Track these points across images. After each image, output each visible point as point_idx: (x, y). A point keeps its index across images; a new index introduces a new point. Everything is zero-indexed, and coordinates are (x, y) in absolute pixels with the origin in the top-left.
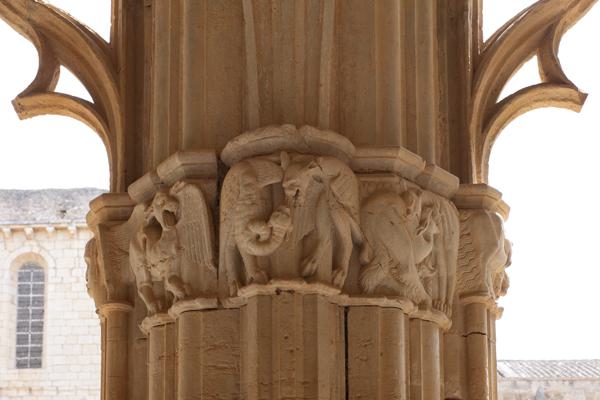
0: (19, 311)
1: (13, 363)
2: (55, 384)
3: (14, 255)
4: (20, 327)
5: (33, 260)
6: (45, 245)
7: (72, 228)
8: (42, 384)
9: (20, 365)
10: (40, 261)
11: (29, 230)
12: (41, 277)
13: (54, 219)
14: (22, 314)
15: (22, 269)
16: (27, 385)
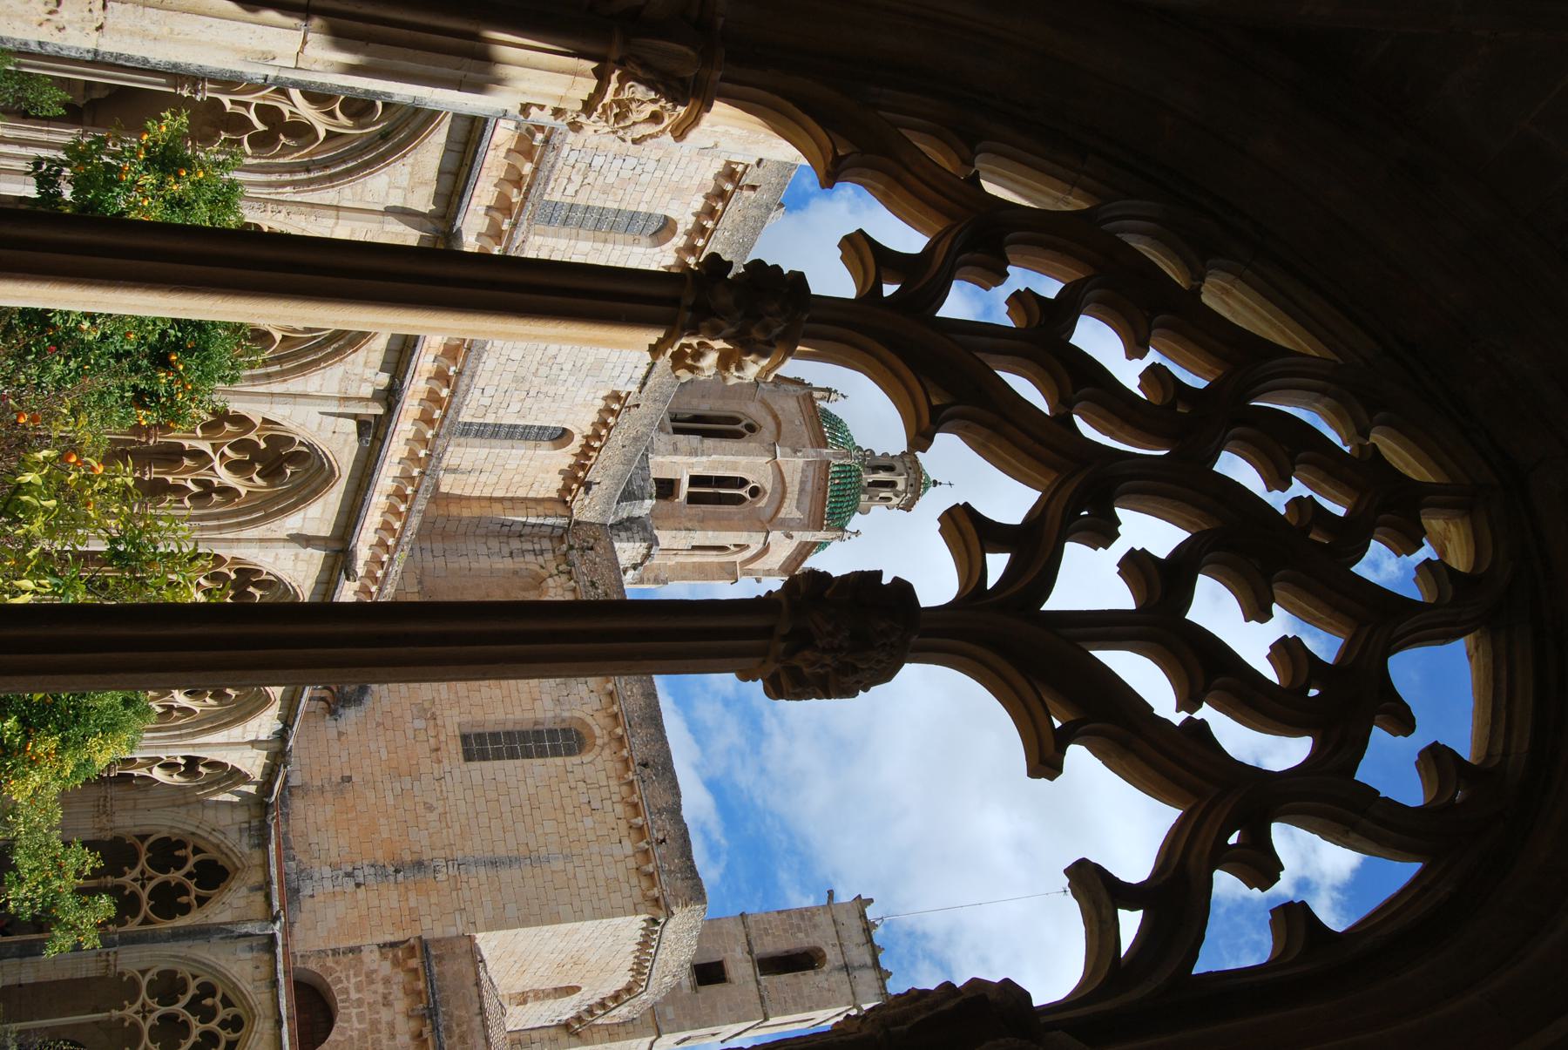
0: (528, 732)
1: (466, 730)
2: (447, 775)
3: (589, 720)
4: (509, 734)
5: (588, 741)
6: (607, 753)
7: (630, 776)
8: (446, 761)
9: (465, 738)
10: (588, 748)
11: (619, 731)
12: (570, 752)
13: (637, 757)
14: (524, 735)
15: (576, 731)
16: (443, 746)
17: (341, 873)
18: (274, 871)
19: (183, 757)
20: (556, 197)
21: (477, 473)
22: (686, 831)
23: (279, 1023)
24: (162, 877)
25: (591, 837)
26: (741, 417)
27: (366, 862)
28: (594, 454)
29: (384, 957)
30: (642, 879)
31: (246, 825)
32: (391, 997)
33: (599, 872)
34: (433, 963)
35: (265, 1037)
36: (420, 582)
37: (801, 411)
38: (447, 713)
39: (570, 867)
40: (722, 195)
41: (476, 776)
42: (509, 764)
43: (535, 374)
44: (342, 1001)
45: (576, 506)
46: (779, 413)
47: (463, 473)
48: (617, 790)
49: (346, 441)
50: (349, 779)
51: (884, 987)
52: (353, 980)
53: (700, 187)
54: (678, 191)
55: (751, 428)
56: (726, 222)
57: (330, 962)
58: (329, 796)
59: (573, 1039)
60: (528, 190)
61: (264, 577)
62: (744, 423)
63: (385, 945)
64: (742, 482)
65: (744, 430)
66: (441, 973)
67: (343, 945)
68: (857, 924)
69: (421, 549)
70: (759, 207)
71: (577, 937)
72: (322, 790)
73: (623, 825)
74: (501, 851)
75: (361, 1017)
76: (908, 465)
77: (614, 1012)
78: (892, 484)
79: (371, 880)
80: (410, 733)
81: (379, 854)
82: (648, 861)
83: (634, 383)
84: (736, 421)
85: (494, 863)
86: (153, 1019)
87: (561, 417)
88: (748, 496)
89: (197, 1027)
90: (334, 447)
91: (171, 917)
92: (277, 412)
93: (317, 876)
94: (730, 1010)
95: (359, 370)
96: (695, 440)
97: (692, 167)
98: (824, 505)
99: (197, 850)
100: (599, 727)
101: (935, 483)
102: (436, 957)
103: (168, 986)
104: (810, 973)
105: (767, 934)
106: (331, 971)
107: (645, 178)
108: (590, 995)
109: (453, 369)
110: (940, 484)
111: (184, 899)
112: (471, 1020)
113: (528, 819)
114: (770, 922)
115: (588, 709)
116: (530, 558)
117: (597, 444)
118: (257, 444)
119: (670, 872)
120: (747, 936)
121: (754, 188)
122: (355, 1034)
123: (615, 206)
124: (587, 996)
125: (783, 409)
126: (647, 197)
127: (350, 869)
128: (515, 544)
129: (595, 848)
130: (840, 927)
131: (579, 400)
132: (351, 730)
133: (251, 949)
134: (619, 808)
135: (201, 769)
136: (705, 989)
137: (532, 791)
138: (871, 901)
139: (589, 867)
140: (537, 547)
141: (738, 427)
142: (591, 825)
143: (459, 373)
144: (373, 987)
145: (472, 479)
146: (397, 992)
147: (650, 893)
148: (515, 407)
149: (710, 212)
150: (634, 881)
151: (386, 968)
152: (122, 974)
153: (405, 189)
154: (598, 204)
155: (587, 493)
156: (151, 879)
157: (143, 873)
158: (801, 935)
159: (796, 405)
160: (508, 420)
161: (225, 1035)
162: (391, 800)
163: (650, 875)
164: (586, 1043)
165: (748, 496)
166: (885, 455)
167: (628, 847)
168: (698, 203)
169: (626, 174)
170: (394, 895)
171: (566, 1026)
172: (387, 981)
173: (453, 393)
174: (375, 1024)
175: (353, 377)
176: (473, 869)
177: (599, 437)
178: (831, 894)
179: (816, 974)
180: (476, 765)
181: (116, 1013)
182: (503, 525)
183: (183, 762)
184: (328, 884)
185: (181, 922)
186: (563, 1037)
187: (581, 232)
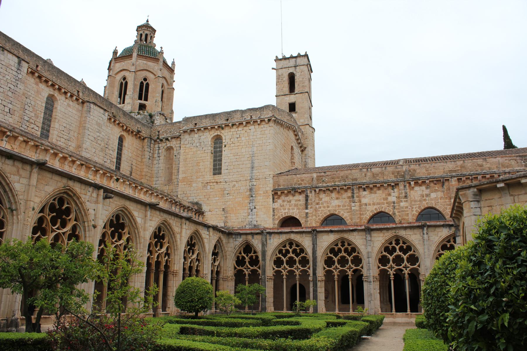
1: (212, 173)
3: (212, 136)
4: (214, 161)
8: (221, 180)
9: (214, 174)
14: (215, 157)
17: (251, 213)
18: (248, 232)
19: (212, 256)
20: (39, 133)
22: (249, 109)
23: (292, 232)
24: (247, 263)
25: (247, 138)
26: (120, 82)
27: (248, 205)
28: (128, 129)
29: (276, 202)
30: (262, 124)
31: (234, 239)
32: (288, 200)
33: (258, 137)
34: (280, 188)
35: (296, 236)
36: (166, 185)
38: (206, 179)
39: (256, 145)
40: (40, 77)
41: (226, 171)
42: (223, 161)
43: (100, 145)
44: (288, 214)
45: (145, 136)
46: (120, 69)
48: (234, 129)
49: (112, 203)
50: (223, 209)
51: (302, 56)
52: (282, 211)
53: (37, 84)
54: (38, 92)
55: (124, 79)
56: (50, 77)
57: (276, 217)
58: (228, 215)
59: (306, 150)
60: (29, 139)
61: (157, 230)
62: (123, 81)
63: (273, 201)
64: (142, 83)
65: (125, 81)
66: (283, 185)
67: (272, 213)
68: (283, 61)
69: (156, 184)
70: (45, 65)
71: (277, 145)
72: (226, 217)
73: (245, 128)
74: (249, 165)
75: (293, 209)
76: (141, 29)
77: (300, 137)
78: (146, 35)
79: (254, 204)
80: (212, 190)
81: (246, 201)
82: (257, 121)
83: (105, 113)
84: (122, 83)
85: (253, 168)
86: (287, 267)
87: (115, 138)
89: (291, 255)
90: (114, 206)
91: (259, 261)
92: (101, 224)
93: (251, 220)
94: (303, 103)
95: (87, 197)
96: (126, 97)
97: (29, 87)
98: (151, 57)
99: (240, 253)
100: (214, 133)
101: (147, 21)
102: (278, 186)
103: (278, 262)
104: (296, 77)
105: (283, 89)
106: (279, 217)
107: (33, 103)
108: (294, 144)
109: (93, 169)
111: (254, 257)
112: (297, 178)
113: (240, 157)
114: (279, 88)
115: (209, 136)
116: (160, 151)
117: (125, 127)
118: (112, 231)
119: (261, 115)
120: (282, 95)
121: (37, 66)
122: (298, 211)
123: (43, 114)
124: (294, 144)
126: (40, 103)
127: (250, 210)
128: (156, 155)
129: (251, 137)
130: (283, 67)
131: (110, 132)
132: (209, 208)
133: (270, 239)
134: (240, 129)
135: (216, 251)
136: (296, 110)
137: (232, 155)
138: (277, 57)
139: (257, 139)
140: (157, 149)
141: (124, 83)
142: (244, 138)
143: (95, 167)
144: (285, 205)
145: (134, 167)
146: (287, 198)
147: (267, 122)
148: (111, 152)
149: (46, 82)
150: (262, 126)
151: (280, 201)
152: (274, 275)
153: (20, 178)
154: (42, 119)
155: (141, 132)
156: (247, 266)
157: (245, 269)
158: (284, 79)
159: (118, 63)
160: (115, 154)
161: (294, 247)
162: (231, 197)
163: (261, 121)
164: (308, 146)
165: (146, 82)
166: (137, 37)
167: (252, 127)
168: (42, 86)
169: (31, 109)
170: (259, 198)
171: (302, 151)
172: (284, 201)
173: (102, 169)
174: (296, 205)
175: (90, 199)
176: (253, 174)
177: (123, 126)
178: (273, 69)
179: (296, 76)
180: (223, 171)
181: (284, 277)
183: (214, 256)
184: (254, 217)
185: (260, 258)
186: (305, 152)
187: (52, 126)
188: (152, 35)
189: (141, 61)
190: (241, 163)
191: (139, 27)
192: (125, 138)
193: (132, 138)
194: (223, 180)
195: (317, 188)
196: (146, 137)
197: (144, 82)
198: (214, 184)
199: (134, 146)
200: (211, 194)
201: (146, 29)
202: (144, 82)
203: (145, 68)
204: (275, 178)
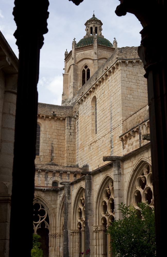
16: (94, 140)
21: (53, 145)
37: (68, 61)
47: (53, 148)
63: (123, 148)
64: (84, 71)
74: (109, 117)
78: (91, 28)
88: (87, 69)
100: (92, 96)
101: (94, 16)
110: (94, 14)
125: (69, 66)
128: (76, 130)
129: (110, 88)
140: (77, 124)
165: (87, 69)
172: (129, 146)
182: (71, 135)
188: (96, 25)
189: (79, 53)
190: (105, 117)
191: (86, 24)
192: (40, 124)
193: (49, 122)
194: (97, 138)
195: (145, 121)
196: (66, 117)
197: (85, 69)
198: (94, 143)
199: (53, 128)
200: (93, 154)
201: (90, 23)
202: (85, 69)
203: (84, 58)
204: (124, 122)
